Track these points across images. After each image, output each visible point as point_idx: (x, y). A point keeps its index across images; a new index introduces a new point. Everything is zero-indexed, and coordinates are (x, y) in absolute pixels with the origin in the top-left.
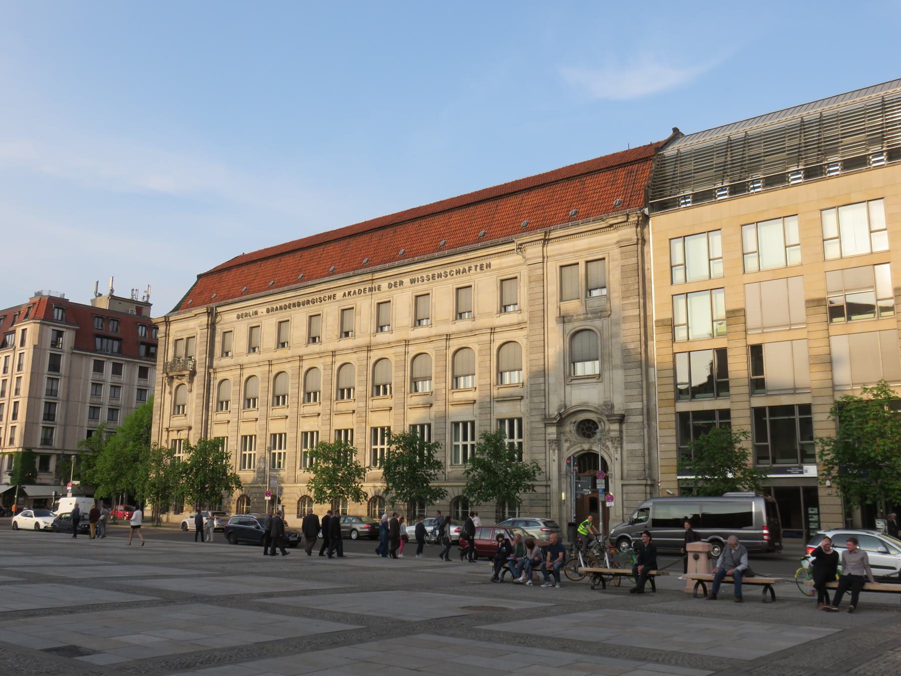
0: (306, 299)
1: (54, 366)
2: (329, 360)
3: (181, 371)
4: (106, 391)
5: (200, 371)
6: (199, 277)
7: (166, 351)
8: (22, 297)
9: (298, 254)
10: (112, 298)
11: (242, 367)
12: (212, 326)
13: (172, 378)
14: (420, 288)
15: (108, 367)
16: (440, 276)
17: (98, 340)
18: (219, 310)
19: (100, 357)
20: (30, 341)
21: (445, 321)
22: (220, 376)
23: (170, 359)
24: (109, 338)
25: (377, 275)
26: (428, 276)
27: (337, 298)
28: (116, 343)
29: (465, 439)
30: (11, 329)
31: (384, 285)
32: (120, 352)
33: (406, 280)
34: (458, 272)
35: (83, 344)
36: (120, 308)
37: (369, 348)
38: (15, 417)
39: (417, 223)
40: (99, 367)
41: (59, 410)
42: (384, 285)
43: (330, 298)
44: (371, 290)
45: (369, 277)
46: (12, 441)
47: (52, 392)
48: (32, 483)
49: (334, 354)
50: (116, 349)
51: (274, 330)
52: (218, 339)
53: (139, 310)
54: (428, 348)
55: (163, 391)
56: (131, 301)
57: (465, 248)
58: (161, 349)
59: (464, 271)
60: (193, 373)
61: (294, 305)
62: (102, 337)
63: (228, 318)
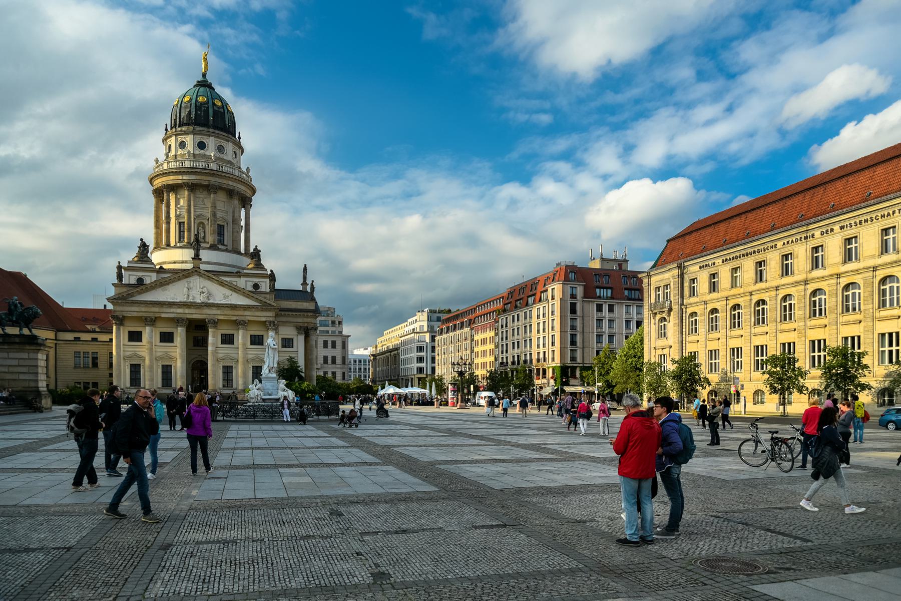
0: (752, 250)
1: (573, 310)
2: (773, 293)
3: (662, 310)
4: (605, 324)
5: (675, 308)
6: (668, 241)
7: (650, 296)
8: (551, 268)
9: (743, 217)
10: (603, 260)
11: (706, 303)
12: (682, 276)
13: (656, 314)
14: (849, 233)
15: (605, 308)
16: (866, 221)
17: (598, 290)
18: (686, 264)
19: (600, 301)
20: (558, 295)
21: (873, 257)
22: (690, 310)
23: (653, 301)
24: (604, 288)
25: (810, 227)
26: (855, 223)
27: (778, 247)
28: (609, 291)
29: (891, 345)
30: (544, 289)
31: (817, 234)
32: (612, 298)
33: (836, 228)
34: (883, 216)
35: (589, 294)
36: (608, 266)
37: (806, 282)
38: (553, 344)
39: (844, 181)
40: (599, 308)
41: (578, 339)
42: (817, 234)
43: (772, 247)
44: (806, 238)
45: (805, 228)
46: (553, 360)
47: (573, 327)
48: (568, 385)
49: (777, 288)
50: (609, 295)
51: (728, 274)
52: (686, 284)
53: (620, 266)
54: (857, 279)
55: (650, 323)
56: (614, 260)
57: (889, 196)
58: (646, 295)
59: (889, 215)
60: (670, 310)
61: (743, 255)
62: (600, 288)
63: (693, 269)
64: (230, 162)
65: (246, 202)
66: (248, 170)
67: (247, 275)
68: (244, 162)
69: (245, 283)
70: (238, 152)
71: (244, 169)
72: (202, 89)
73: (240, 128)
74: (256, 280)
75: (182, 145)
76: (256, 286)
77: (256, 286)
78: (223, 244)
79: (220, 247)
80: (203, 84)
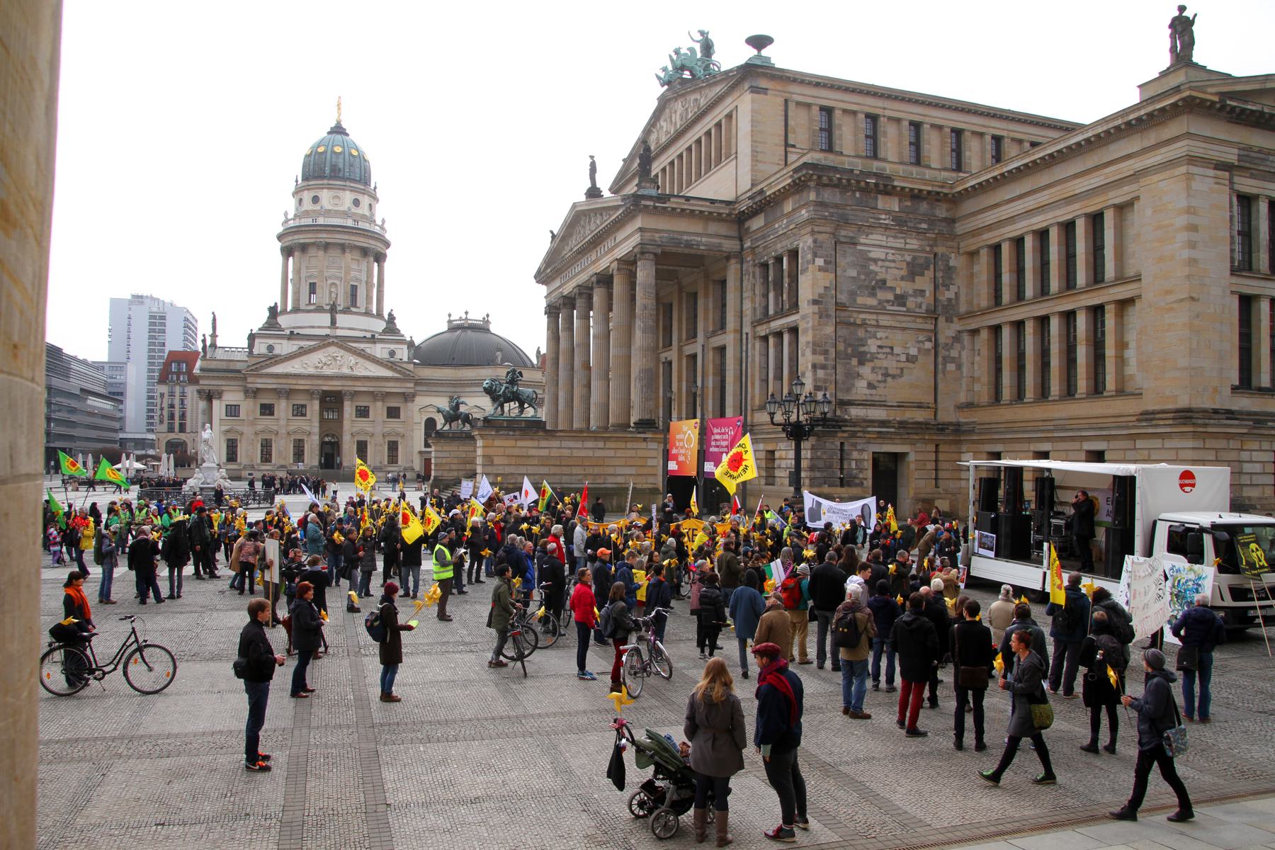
64: (363, 216)
65: (380, 258)
66: (383, 221)
67: (382, 341)
68: (380, 213)
69: (380, 351)
70: (372, 202)
71: (379, 222)
72: (339, 137)
73: (377, 178)
74: (393, 347)
75: (316, 200)
76: (392, 353)
77: (392, 353)
78: (355, 306)
79: (353, 309)
80: (338, 130)
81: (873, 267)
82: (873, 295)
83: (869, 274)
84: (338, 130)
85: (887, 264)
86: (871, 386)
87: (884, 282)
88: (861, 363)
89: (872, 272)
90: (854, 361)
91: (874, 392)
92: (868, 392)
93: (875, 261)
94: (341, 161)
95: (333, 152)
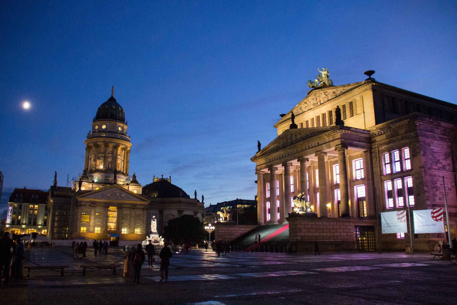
80: (112, 100)
81: (436, 155)
82: (437, 165)
83: (435, 157)
84: (112, 100)
85: (439, 154)
86: (440, 199)
87: (439, 160)
88: (436, 190)
89: (435, 157)
90: (435, 190)
91: (441, 201)
92: (439, 201)
93: (436, 153)
94: (115, 112)
95: (112, 108)
